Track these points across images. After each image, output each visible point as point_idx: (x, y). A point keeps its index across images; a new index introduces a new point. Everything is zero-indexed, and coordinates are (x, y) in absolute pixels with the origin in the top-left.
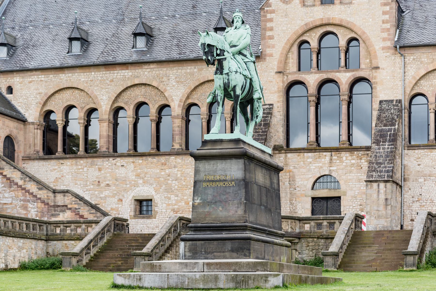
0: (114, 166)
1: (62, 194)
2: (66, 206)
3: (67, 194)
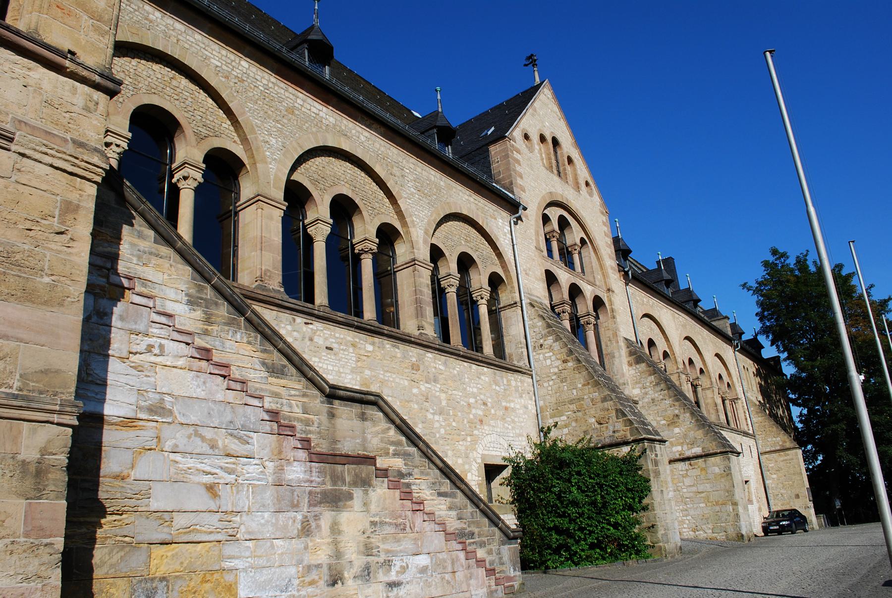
0: (308, 343)
1: (356, 408)
2: (370, 460)
3: (372, 412)
